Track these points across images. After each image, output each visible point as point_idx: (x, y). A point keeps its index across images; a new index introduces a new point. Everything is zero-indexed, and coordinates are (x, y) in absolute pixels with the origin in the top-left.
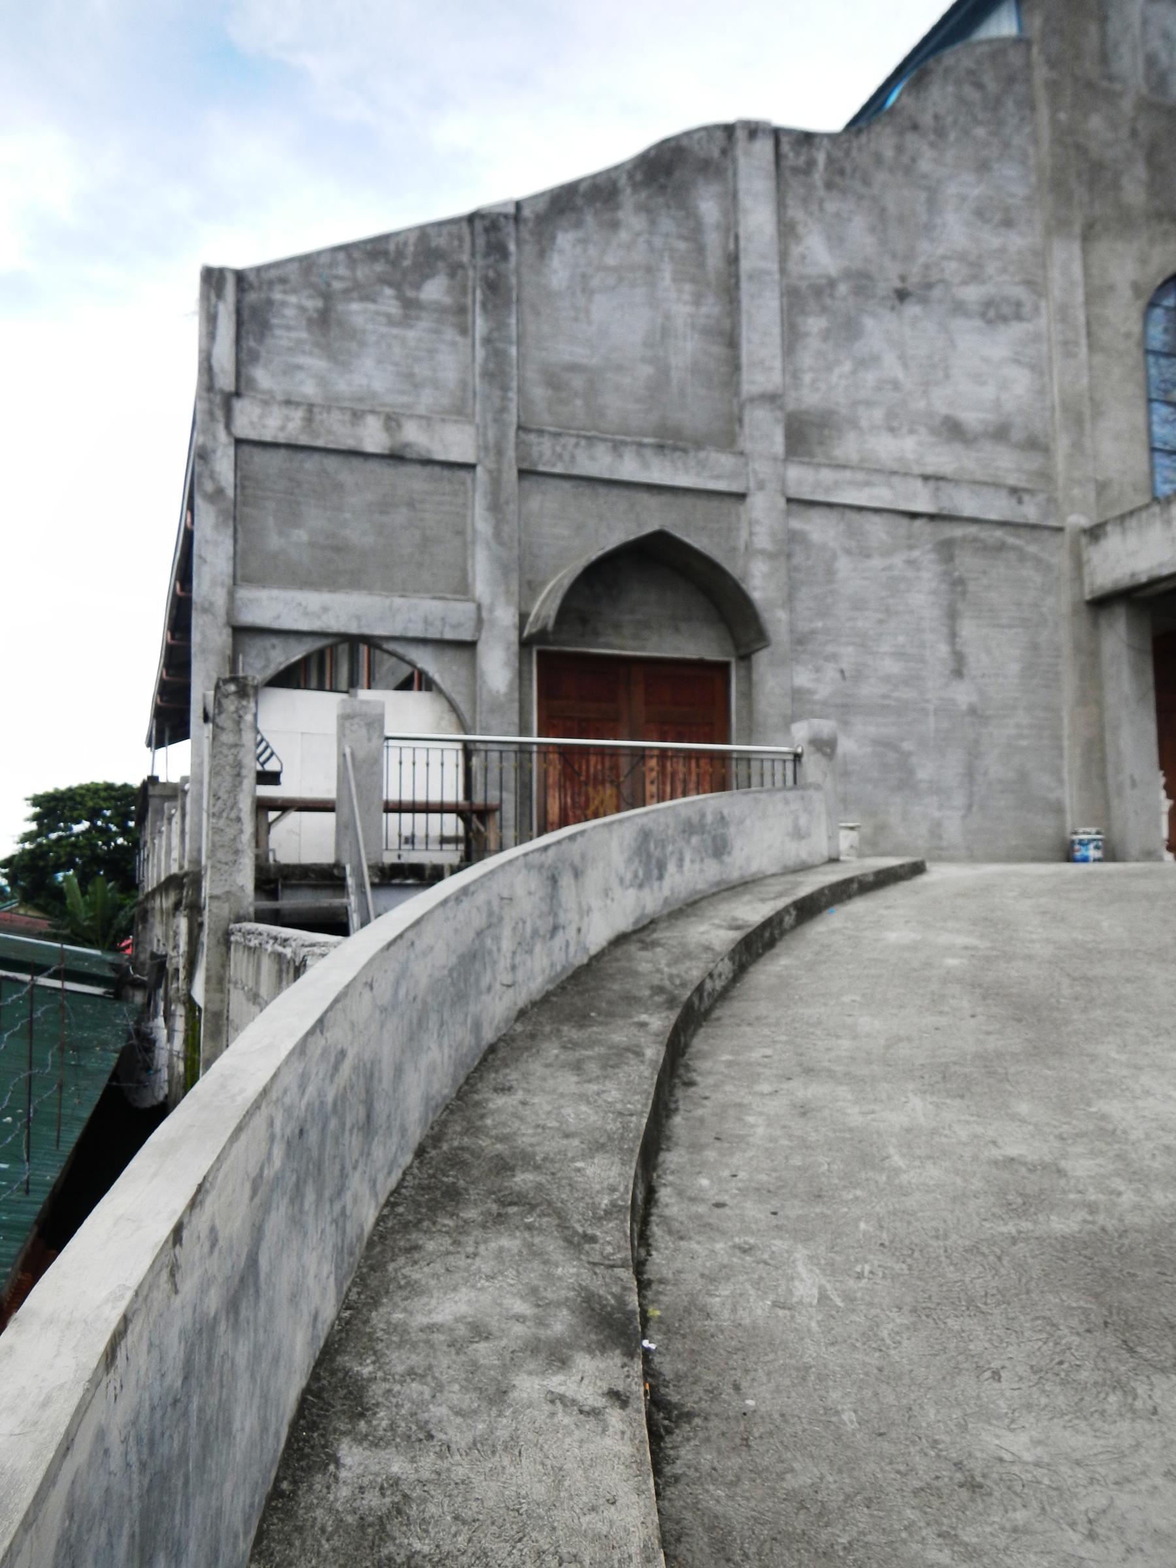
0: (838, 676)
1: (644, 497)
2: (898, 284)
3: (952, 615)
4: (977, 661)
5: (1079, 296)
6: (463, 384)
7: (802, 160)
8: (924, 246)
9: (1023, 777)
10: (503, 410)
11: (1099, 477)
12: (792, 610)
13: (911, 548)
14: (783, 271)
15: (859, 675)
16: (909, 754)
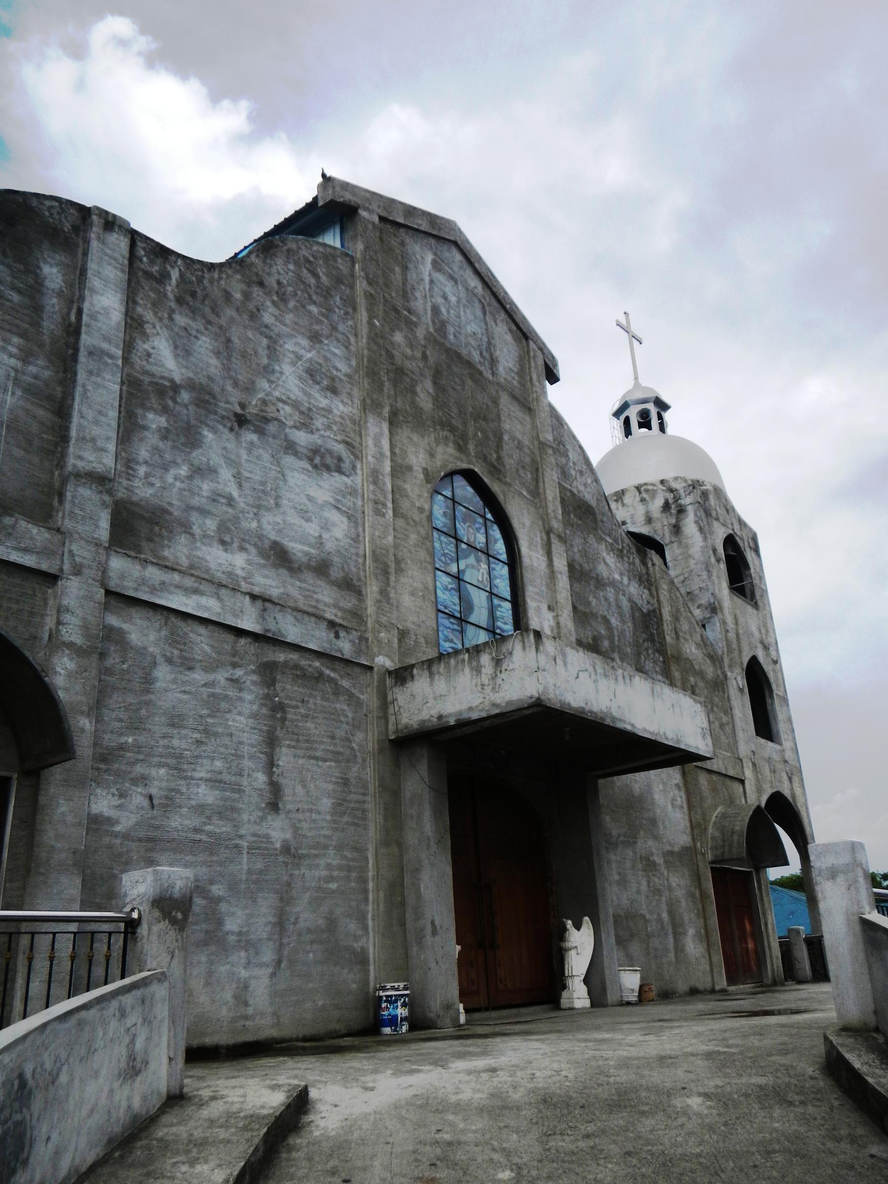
0: (146, 803)
2: (239, 410)
3: (271, 742)
4: (294, 791)
5: (387, 467)
8: (263, 384)
9: (332, 924)
11: (401, 627)
12: (99, 720)
13: (235, 665)
14: (126, 359)
16: (220, 899)
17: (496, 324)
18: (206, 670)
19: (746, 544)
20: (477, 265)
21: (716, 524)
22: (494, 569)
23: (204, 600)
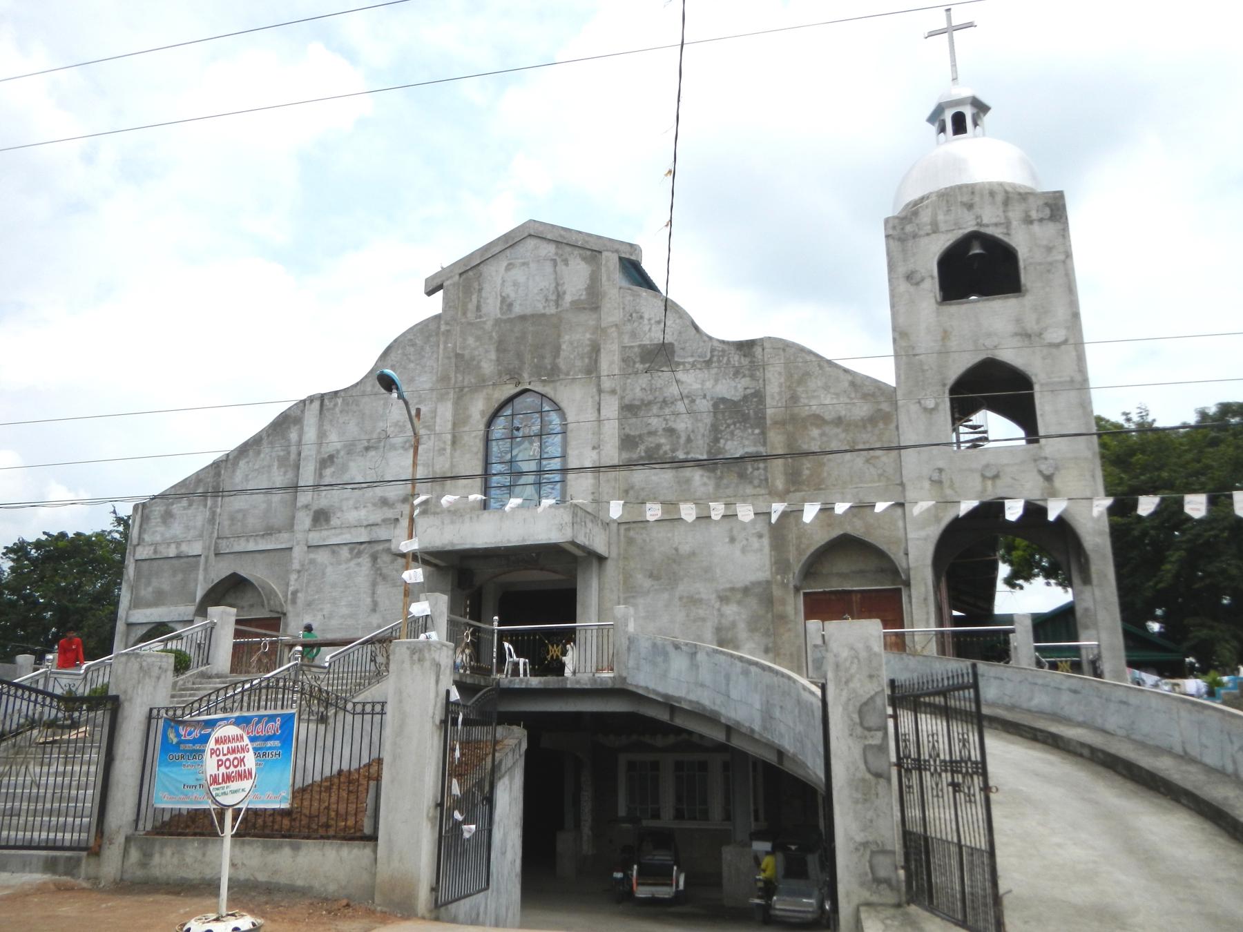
1: (257, 555)
2: (366, 444)
3: (374, 585)
4: (384, 604)
6: (203, 525)
7: (331, 405)
10: (213, 533)
15: (331, 616)
17: (566, 264)
18: (346, 563)
19: (1015, 223)
20: (549, 237)
21: (924, 241)
22: (545, 442)
23: (344, 536)
